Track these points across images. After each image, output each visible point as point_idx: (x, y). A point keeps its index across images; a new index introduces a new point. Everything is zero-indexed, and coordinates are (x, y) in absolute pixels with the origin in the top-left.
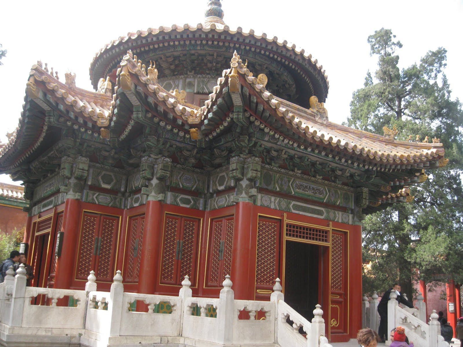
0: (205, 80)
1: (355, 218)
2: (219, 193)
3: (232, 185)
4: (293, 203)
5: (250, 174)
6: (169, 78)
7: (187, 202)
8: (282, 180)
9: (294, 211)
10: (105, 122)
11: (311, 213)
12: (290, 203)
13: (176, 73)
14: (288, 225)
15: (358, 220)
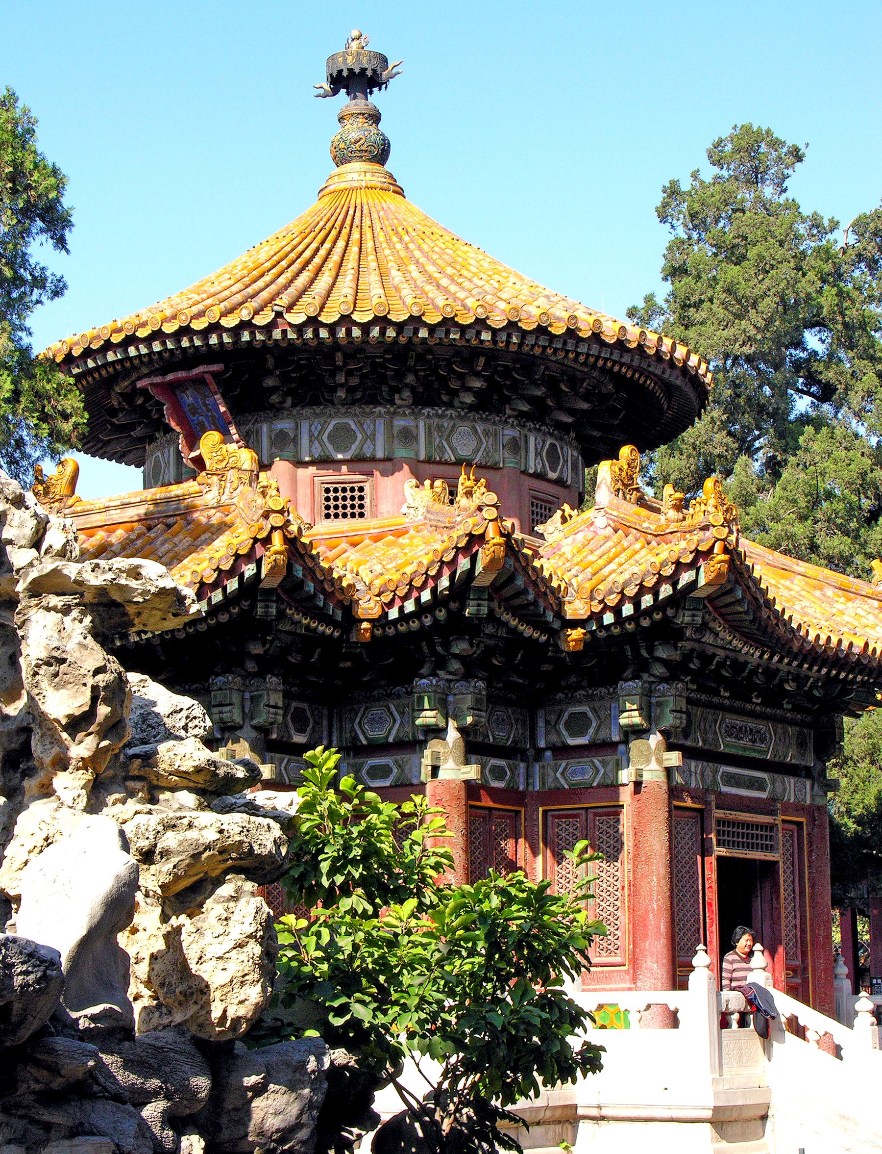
0: (446, 425)
1: (816, 787)
2: (562, 751)
3: (616, 738)
4: (724, 768)
5: (669, 720)
6: (343, 410)
7: (499, 773)
8: (706, 719)
9: (725, 789)
10: (371, 609)
11: (748, 788)
12: (716, 772)
13: (358, 395)
14: (719, 822)
15: (820, 793)
